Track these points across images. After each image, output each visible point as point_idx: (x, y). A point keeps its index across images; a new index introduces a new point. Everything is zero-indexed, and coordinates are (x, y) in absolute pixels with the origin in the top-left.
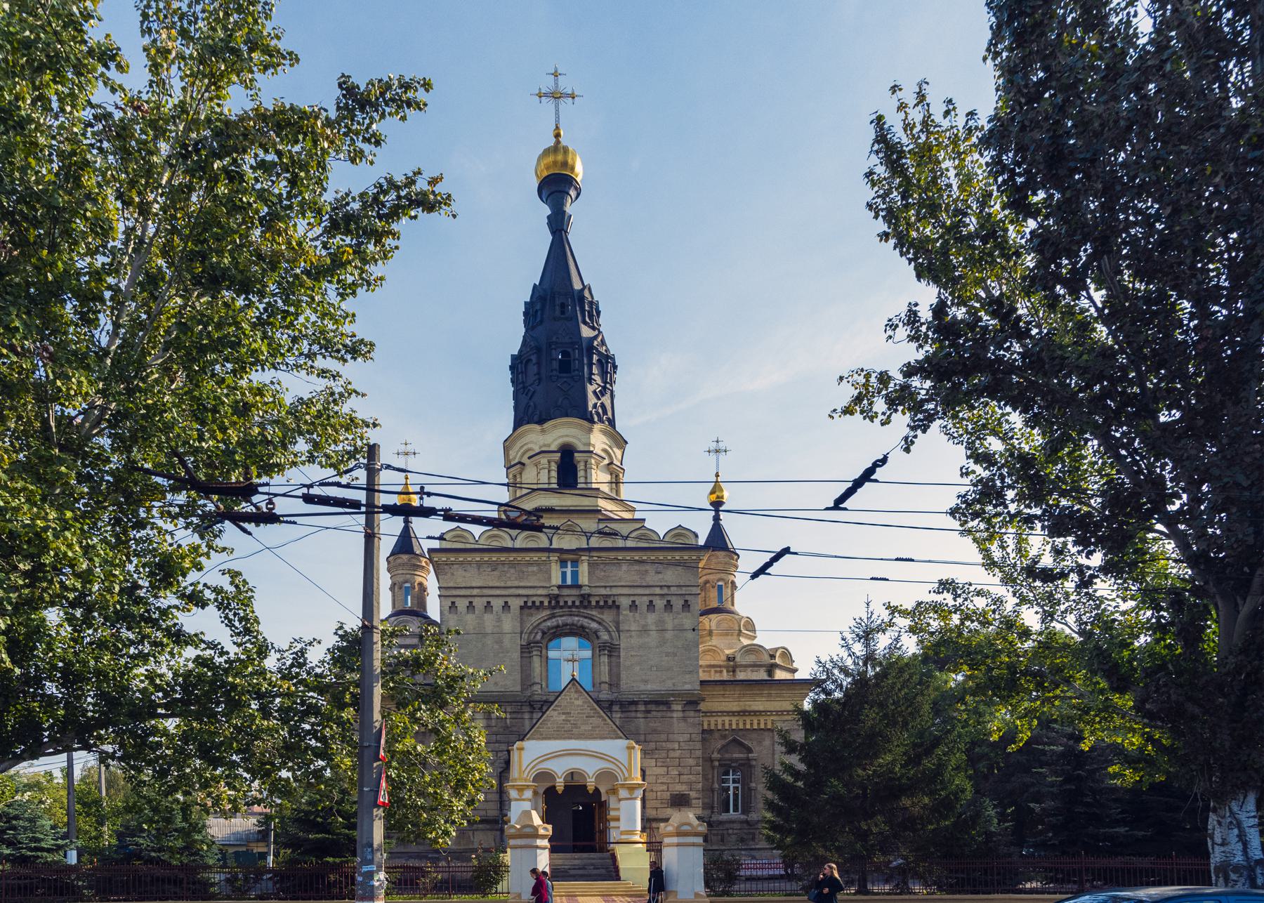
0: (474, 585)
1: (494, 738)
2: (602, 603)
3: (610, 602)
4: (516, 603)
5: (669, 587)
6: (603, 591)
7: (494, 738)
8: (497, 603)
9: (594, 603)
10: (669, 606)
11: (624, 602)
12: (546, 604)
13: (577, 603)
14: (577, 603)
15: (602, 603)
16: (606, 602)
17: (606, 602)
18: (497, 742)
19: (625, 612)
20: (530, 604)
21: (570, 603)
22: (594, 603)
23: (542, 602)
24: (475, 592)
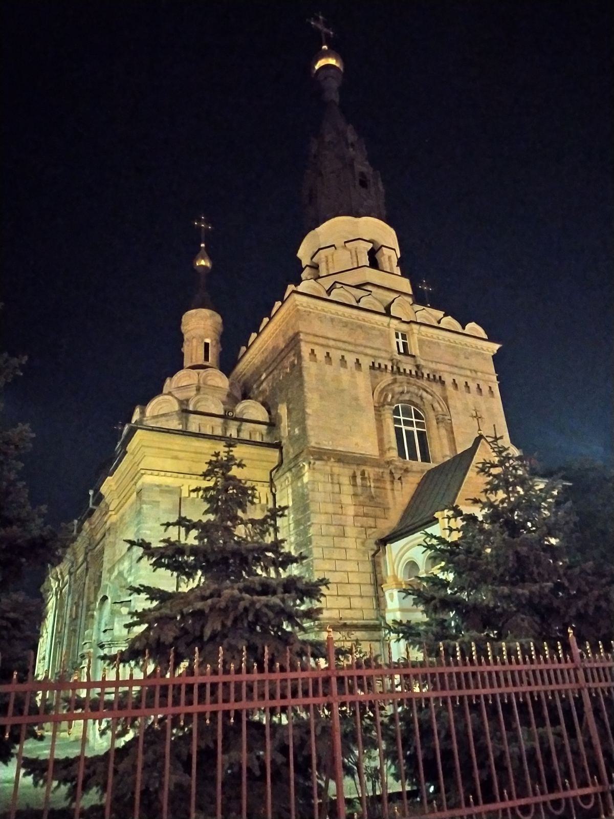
0: (330, 335)
1: (361, 510)
2: (431, 377)
3: (437, 377)
4: (366, 362)
5: (476, 372)
6: (433, 366)
7: (361, 510)
8: (351, 359)
9: (426, 376)
10: (479, 389)
11: (448, 380)
12: (389, 368)
13: (413, 373)
14: (413, 373)
15: (431, 377)
16: (434, 376)
17: (434, 376)
18: (365, 515)
19: (450, 388)
20: (377, 366)
21: (408, 372)
22: (426, 376)
23: (386, 366)
24: (331, 343)
